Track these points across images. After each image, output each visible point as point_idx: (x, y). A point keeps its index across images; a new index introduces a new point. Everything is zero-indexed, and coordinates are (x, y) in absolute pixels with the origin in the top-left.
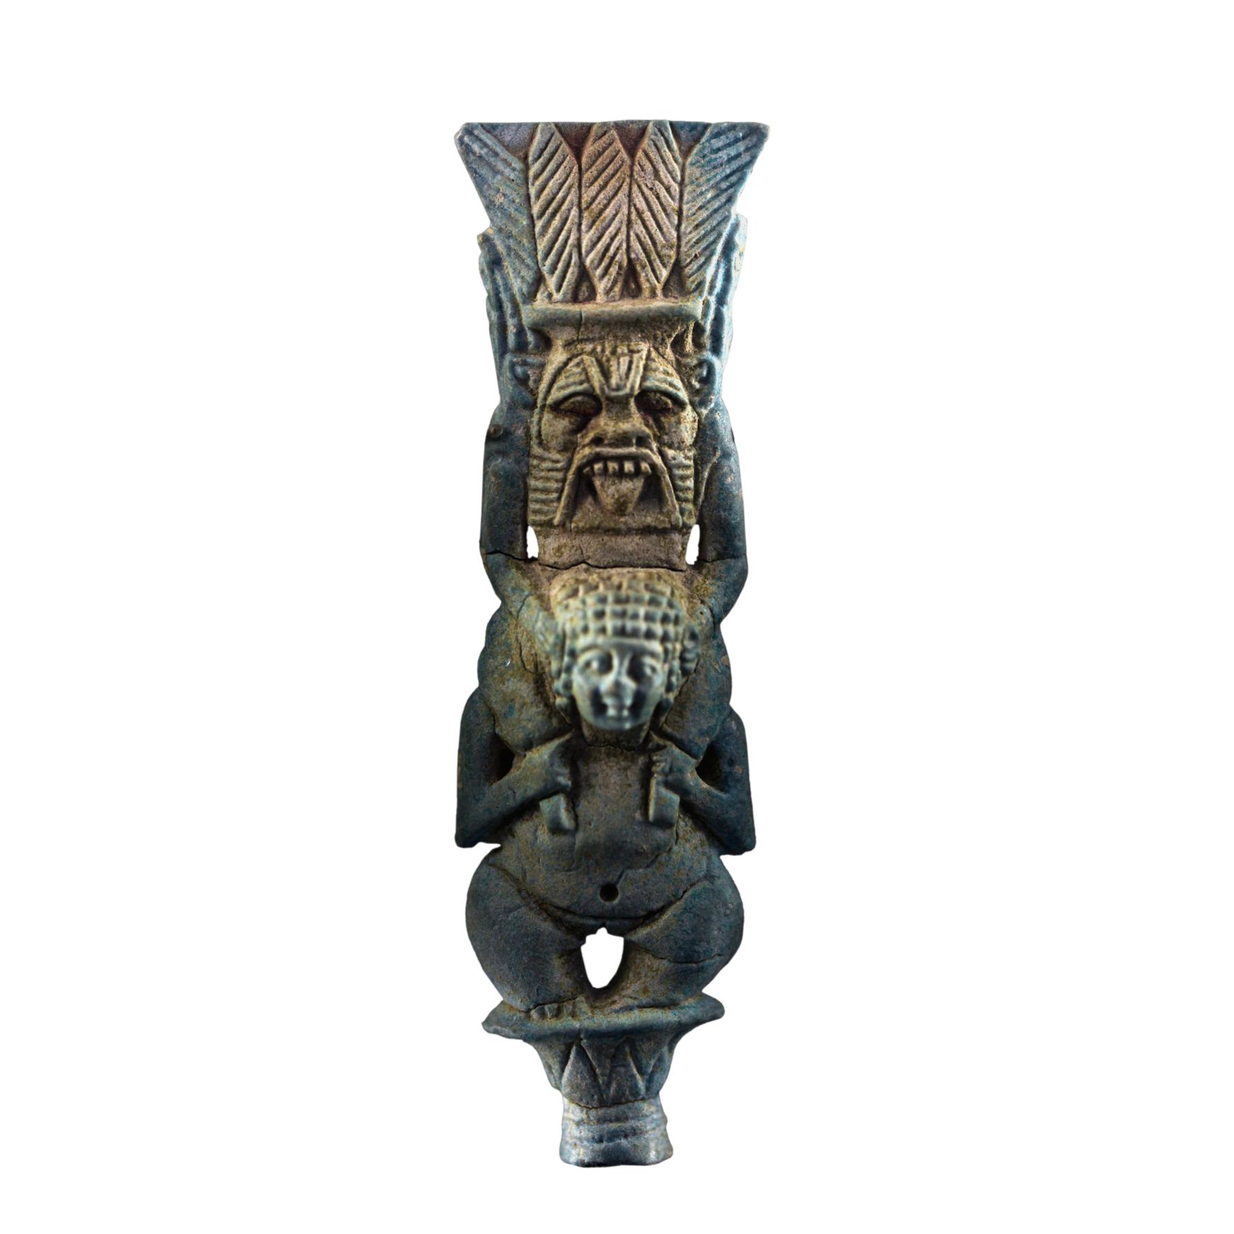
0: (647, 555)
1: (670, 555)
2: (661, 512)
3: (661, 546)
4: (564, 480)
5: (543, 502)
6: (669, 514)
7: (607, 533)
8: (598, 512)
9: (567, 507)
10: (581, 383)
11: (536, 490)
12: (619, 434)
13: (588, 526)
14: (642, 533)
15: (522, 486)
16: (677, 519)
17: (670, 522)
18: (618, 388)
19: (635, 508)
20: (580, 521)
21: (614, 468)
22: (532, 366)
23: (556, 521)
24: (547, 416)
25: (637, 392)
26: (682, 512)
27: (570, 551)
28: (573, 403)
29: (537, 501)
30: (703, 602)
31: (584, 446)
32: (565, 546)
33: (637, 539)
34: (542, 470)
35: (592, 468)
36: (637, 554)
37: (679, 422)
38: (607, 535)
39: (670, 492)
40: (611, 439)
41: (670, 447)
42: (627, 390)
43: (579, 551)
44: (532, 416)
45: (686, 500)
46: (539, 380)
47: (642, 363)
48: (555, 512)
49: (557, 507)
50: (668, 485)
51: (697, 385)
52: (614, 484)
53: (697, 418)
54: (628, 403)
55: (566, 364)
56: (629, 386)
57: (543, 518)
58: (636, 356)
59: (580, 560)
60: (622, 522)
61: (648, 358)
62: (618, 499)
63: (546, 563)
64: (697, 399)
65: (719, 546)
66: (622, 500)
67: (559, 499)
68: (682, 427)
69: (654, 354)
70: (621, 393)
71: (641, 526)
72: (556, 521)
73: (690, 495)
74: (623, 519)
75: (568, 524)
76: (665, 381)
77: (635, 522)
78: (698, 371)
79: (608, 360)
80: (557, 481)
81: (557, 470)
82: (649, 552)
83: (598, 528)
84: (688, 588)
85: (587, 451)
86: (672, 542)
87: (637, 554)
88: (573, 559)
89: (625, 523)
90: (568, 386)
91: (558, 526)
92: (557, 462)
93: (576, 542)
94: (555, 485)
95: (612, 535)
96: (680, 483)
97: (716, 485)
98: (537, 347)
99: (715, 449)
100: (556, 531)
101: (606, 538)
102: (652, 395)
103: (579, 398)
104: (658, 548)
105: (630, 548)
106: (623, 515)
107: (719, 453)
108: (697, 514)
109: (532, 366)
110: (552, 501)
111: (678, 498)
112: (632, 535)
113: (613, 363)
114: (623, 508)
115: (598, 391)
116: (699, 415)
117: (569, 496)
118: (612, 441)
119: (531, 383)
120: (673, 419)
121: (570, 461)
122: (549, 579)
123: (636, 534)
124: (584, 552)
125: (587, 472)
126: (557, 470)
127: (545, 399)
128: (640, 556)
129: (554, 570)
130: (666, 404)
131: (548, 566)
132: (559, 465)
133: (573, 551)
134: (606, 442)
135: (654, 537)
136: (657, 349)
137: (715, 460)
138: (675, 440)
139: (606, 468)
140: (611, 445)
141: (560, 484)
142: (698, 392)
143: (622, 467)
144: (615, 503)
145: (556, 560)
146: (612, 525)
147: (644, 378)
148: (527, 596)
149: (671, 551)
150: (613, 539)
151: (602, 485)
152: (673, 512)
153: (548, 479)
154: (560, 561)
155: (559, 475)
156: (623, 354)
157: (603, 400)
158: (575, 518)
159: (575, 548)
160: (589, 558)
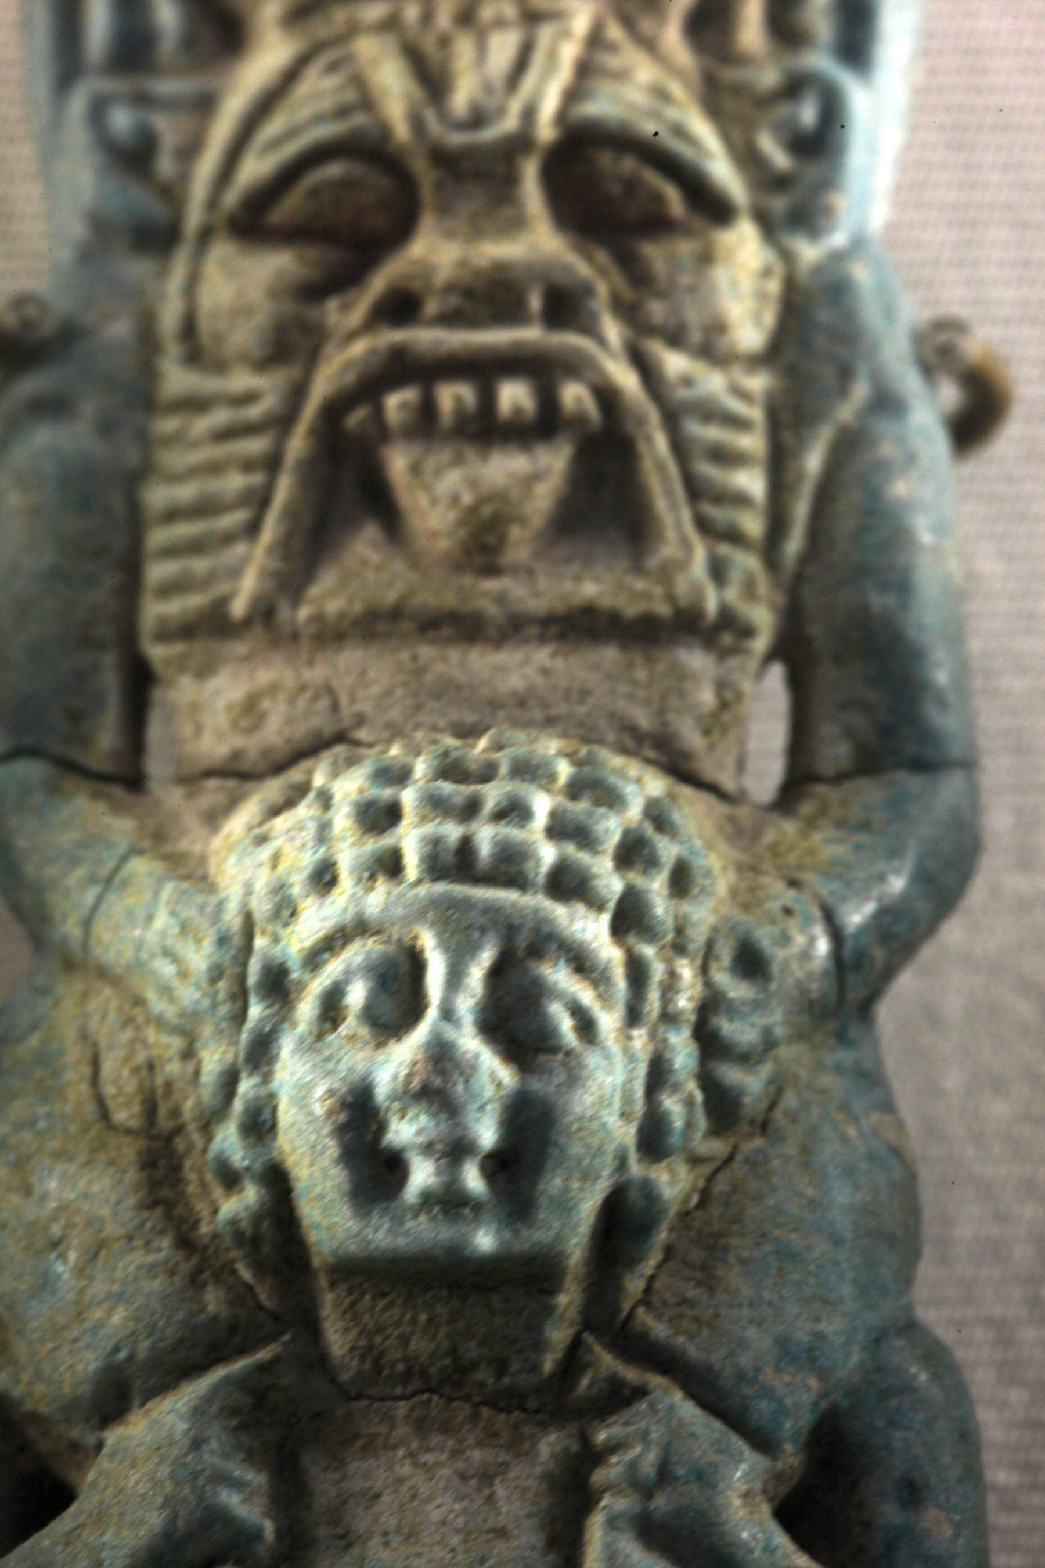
0: (582, 710)
1: (672, 717)
2: (638, 567)
3: (634, 683)
4: (272, 463)
5: (196, 547)
6: (666, 574)
7: (431, 634)
8: (399, 566)
9: (284, 547)
10: (342, 112)
11: (173, 515)
12: (477, 273)
13: (358, 608)
14: (562, 637)
15: (119, 509)
16: (697, 591)
17: (670, 597)
18: (478, 119)
19: (538, 555)
20: (332, 594)
21: (458, 400)
22: (170, 105)
23: (239, 608)
24: (222, 250)
25: (546, 131)
26: (718, 571)
27: (292, 701)
28: (314, 193)
29: (171, 552)
30: (793, 883)
31: (351, 336)
32: (273, 689)
33: (543, 655)
34: (195, 445)
35: (378, 412)
36: (545, 705)
37: (706, 258)
38: (433, 642)
39: (669, 494)
40: (450, 288)
41: (675, 339)
42: (510, 123)
43: (324, 703)
44: (163, 274)
45: (735, 537)
46: (189, 151)
47: (569, 52)
48: (236, 572)
49: (245, 560)
50: (661, 467)
51: (780, 159)
52: (458, 461)
53: (779, 269)
54: (511, 180)
55: (290, 76)
56: (515, 106)
57: (195, 601)
58: (545, 34)
59: (328, 730)
60: (486, 594)
61: (595, 40)
62: (473, 510)
63: (205, 764)
64: (779, 204)
65: (858, 720)
66: (487, 511)
67: (253, 528)
68: (720, 275)
69: (614, 32)
70: (489, 134)
71: (560, 607)
72: (239, 608)
73: (753, 525)
74: (491, 585)
75: (284, 613)
76: (656, 115)
77: (537, 595)
78: (783, 110)
79: (445, 42)
80: (247, 466)
81: (249, 430)
82: (592, 701)
83: (396, 614)
84: (743, 849)
85: (359, 348)
86: (681, 675)
87: (545, 705)
88: (300, 731)
89: (501, 599)
90: (292, 132)
91: (247, 623)
92: (248, 398)
93: (316, 674)
94: (235, 482)
95: (450, 641)
96: (706, 469)
97: (849, 500)
98: (189, 42)
99: (845, 374)
100: (241, 648)
101: (426, 651)
102: (605, 159)
103: (334, 170)
104: (623, 688)
105: (514, 682)
106: (492, 570)
107: (861, 390)
108: (780, 599)
109: (170, 105)
110: (228, 539)
111: (703, 525)
112: (526, 641)
113: (464, 49)
114: (491, 539)
115: (402, 131)
116: (787, 257)
117: (291, 513)
118: (454, 301)
119: (165, 165)
120: (685, 248)
121: (298, 393)
122: (214, 819)
123: (542, 639)
124: (344, 700)
125: (363, 422)
126: (249, 430)
127: (213, 203)
128: (554, 712)
129: (231, 783)
130: (659, 199)
131: (210, 773)
132: (254, 412)
133: (302, 703)
134: (431, 307)
135: (610, 654)
136: (628, 22)
137: (846, 412)
138: (694, 318)
139: (427, 409)
140: (450, 319)
141: (257, 479)
142: (780, 182)
143: (488, 399)
144: (461, 522)
145: (238, 741)
146: (450, 600)
147: (573, 95)
148: (124, 859)
149: (673, 702)
150: (454, 654)
151: (416, 469)
152: (683, 565)
153: (214, 468)
154: (252, 745)
155: (256, 446)
156: (500, 23)
157: (421, 167)
158: (314, 591)
159: (309, 694)
160: (360, 720)
